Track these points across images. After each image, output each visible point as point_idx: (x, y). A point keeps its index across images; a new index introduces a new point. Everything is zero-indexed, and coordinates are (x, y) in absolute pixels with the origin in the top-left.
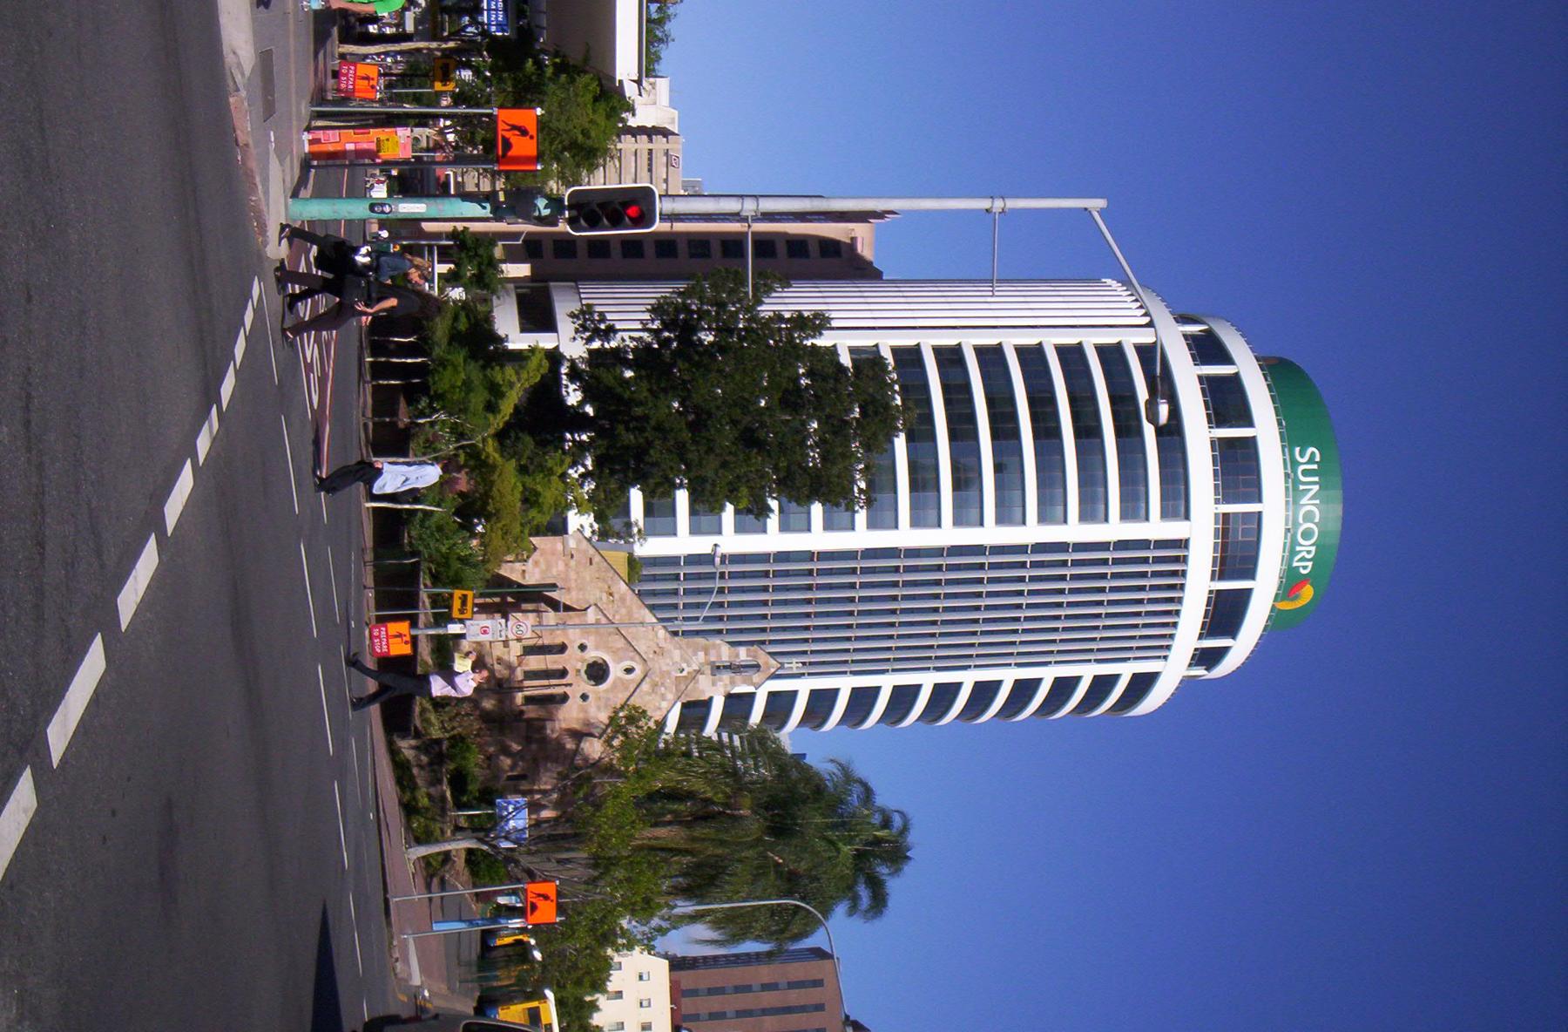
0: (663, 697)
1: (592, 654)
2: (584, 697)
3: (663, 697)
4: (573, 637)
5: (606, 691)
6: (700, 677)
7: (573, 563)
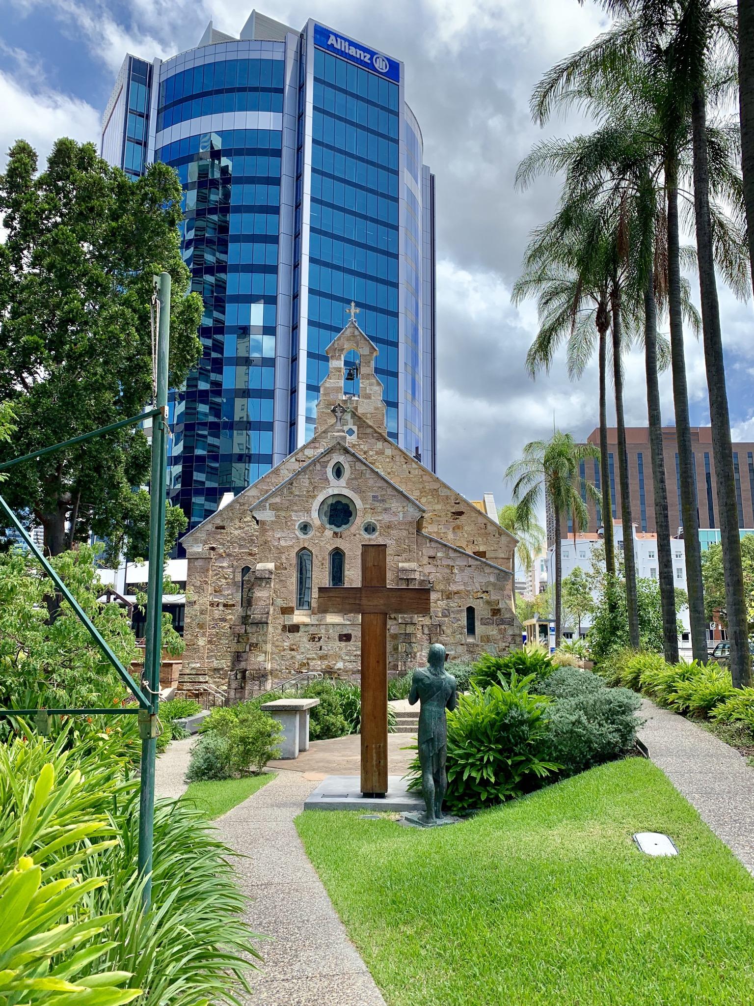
0: (380, 453)
1: (315, 518)
2: (370, 529)
4: (289, 540)
5: (363, 499)
6: (360, 411)
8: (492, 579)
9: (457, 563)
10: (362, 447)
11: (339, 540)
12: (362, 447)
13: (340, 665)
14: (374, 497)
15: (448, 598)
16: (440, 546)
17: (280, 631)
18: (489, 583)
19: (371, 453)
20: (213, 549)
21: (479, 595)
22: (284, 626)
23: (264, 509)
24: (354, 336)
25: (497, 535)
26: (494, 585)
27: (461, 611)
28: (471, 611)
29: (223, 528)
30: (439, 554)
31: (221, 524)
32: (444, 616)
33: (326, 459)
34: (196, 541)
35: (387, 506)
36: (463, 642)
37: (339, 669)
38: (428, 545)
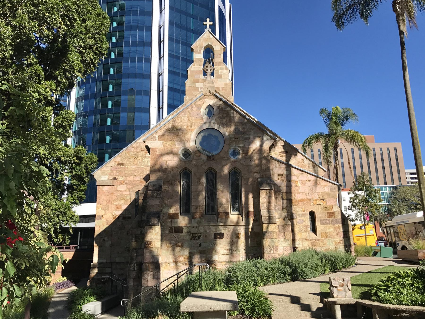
7: (120, 178)
8: (326, 190)
9: (300, 178)
11: (212, 162)
17: (167, 232)
18: (324, 193)
20: (115, 179)
21: (318, 202)
22: (171, 228)
23: (154, 139)
24: (210, 38)
26: (328, 194)
27: (305, 214)
28: (312, 214)
29: (122, 164)
31: (121, 162)
33: (200, 103)
34: (103, 173)
35: (247, 136)
36: (308, 238)
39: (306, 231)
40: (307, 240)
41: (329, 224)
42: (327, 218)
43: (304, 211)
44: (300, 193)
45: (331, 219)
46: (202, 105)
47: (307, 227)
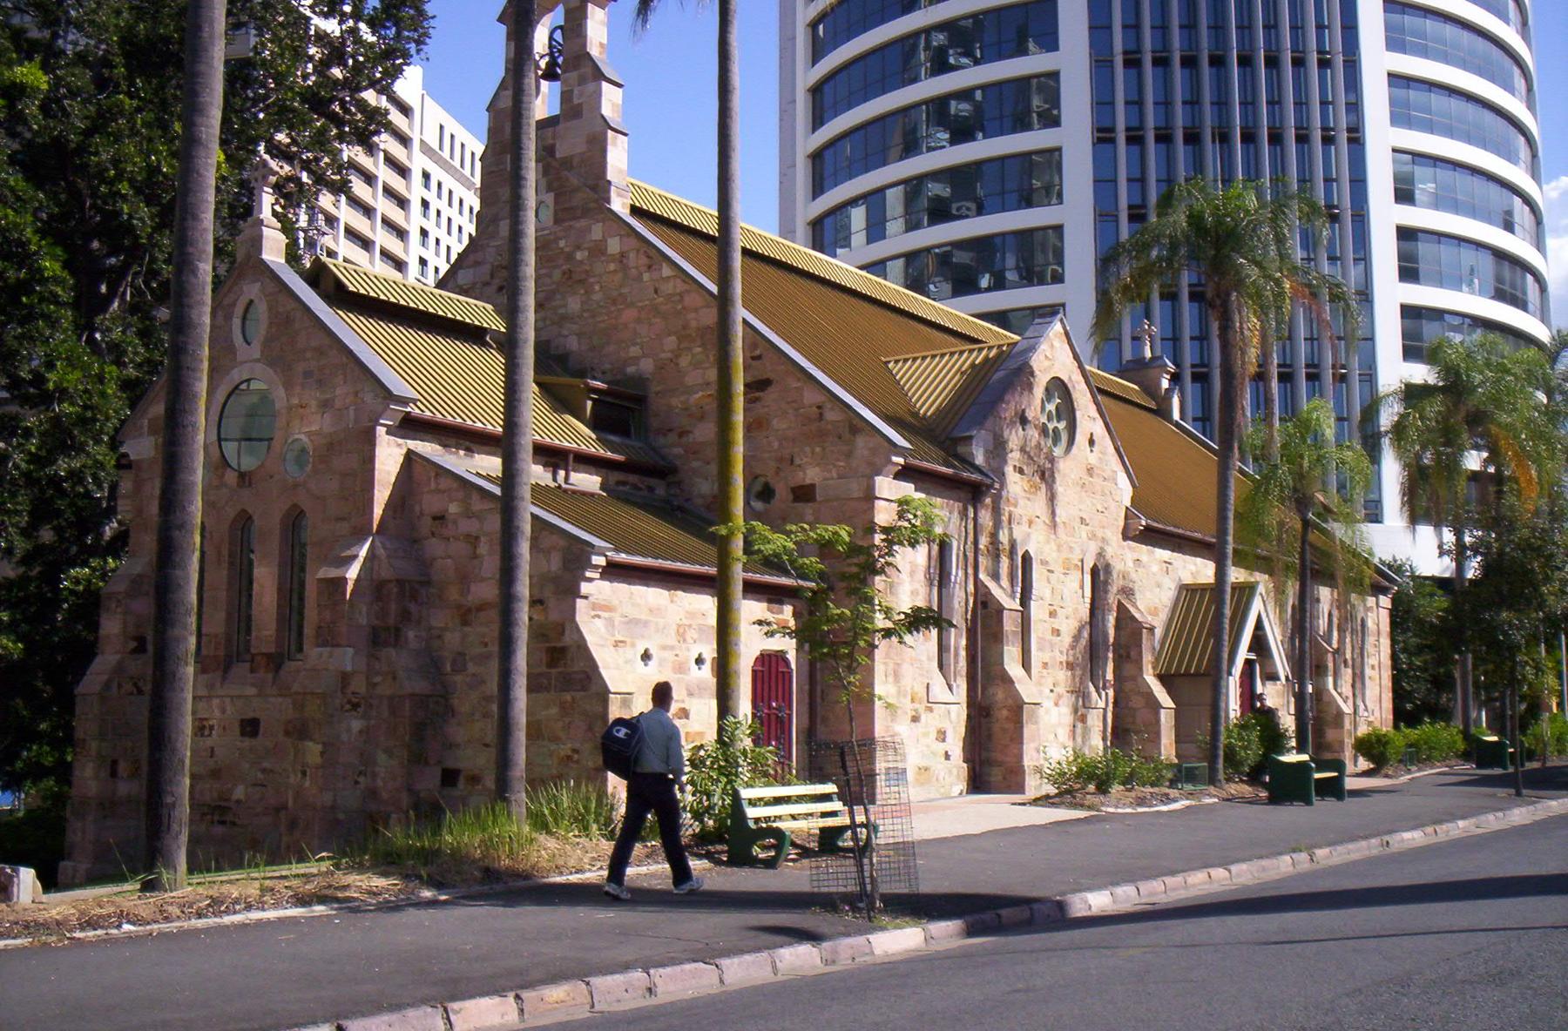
3: (598, 250)
5: (288, 386)
10: (562, 243)
12: (562, 243)
13: (239, 792)
14: (308, 374)
15: (465, 623)
16: (455, 485)
19: (579, 256)
25: (847, 435)
27: (487, 657)
30: (453, 508)
32: (455, 671)
37: (238, 802)
38: (433, 486)
39: (486, 715)
40: (486, 745)
41: (547, 689)
42: (544, 669)
43: (486, 645)
44: (483, 580)
45: (553, 671)
46: (234, 304)
47: (488, 699)
